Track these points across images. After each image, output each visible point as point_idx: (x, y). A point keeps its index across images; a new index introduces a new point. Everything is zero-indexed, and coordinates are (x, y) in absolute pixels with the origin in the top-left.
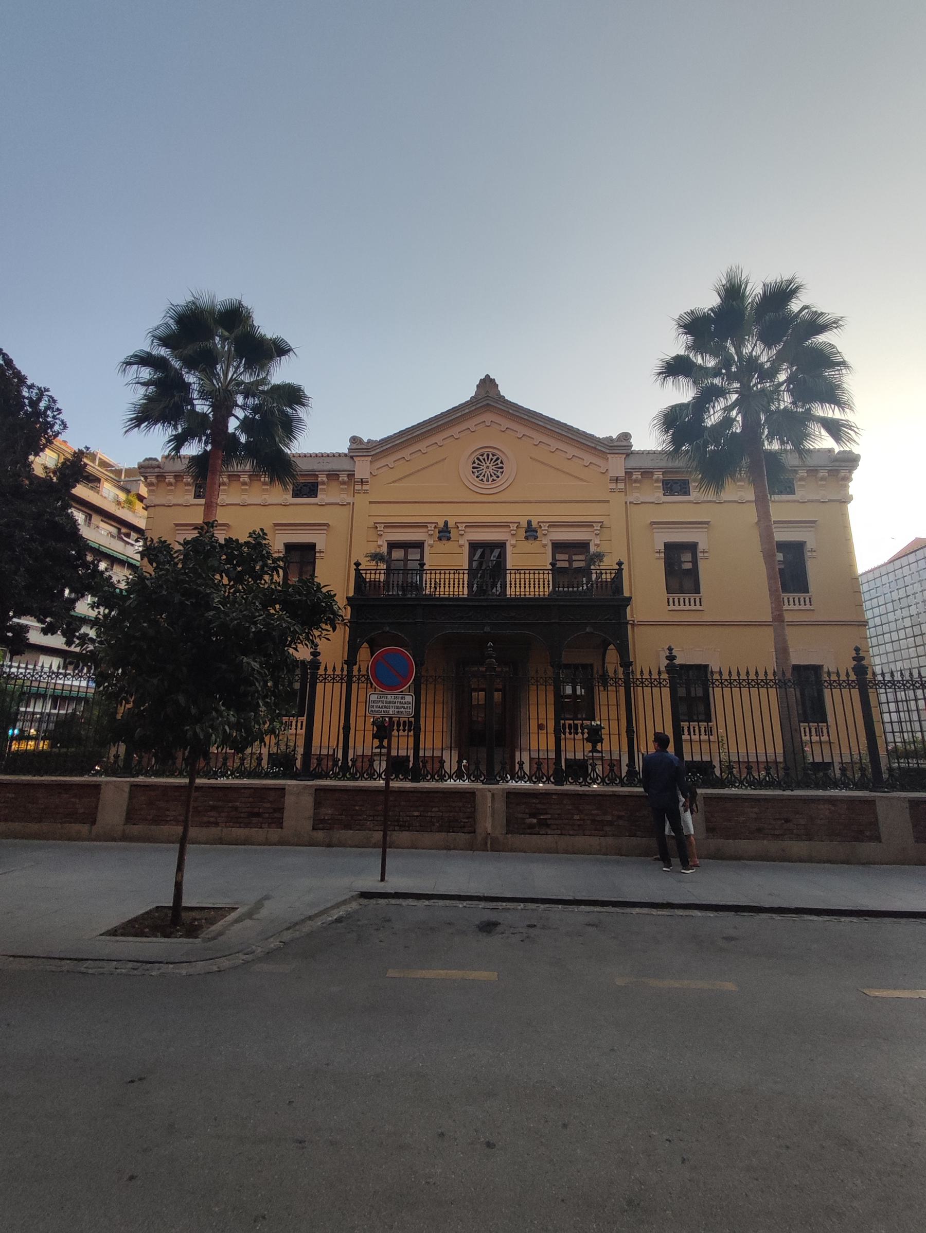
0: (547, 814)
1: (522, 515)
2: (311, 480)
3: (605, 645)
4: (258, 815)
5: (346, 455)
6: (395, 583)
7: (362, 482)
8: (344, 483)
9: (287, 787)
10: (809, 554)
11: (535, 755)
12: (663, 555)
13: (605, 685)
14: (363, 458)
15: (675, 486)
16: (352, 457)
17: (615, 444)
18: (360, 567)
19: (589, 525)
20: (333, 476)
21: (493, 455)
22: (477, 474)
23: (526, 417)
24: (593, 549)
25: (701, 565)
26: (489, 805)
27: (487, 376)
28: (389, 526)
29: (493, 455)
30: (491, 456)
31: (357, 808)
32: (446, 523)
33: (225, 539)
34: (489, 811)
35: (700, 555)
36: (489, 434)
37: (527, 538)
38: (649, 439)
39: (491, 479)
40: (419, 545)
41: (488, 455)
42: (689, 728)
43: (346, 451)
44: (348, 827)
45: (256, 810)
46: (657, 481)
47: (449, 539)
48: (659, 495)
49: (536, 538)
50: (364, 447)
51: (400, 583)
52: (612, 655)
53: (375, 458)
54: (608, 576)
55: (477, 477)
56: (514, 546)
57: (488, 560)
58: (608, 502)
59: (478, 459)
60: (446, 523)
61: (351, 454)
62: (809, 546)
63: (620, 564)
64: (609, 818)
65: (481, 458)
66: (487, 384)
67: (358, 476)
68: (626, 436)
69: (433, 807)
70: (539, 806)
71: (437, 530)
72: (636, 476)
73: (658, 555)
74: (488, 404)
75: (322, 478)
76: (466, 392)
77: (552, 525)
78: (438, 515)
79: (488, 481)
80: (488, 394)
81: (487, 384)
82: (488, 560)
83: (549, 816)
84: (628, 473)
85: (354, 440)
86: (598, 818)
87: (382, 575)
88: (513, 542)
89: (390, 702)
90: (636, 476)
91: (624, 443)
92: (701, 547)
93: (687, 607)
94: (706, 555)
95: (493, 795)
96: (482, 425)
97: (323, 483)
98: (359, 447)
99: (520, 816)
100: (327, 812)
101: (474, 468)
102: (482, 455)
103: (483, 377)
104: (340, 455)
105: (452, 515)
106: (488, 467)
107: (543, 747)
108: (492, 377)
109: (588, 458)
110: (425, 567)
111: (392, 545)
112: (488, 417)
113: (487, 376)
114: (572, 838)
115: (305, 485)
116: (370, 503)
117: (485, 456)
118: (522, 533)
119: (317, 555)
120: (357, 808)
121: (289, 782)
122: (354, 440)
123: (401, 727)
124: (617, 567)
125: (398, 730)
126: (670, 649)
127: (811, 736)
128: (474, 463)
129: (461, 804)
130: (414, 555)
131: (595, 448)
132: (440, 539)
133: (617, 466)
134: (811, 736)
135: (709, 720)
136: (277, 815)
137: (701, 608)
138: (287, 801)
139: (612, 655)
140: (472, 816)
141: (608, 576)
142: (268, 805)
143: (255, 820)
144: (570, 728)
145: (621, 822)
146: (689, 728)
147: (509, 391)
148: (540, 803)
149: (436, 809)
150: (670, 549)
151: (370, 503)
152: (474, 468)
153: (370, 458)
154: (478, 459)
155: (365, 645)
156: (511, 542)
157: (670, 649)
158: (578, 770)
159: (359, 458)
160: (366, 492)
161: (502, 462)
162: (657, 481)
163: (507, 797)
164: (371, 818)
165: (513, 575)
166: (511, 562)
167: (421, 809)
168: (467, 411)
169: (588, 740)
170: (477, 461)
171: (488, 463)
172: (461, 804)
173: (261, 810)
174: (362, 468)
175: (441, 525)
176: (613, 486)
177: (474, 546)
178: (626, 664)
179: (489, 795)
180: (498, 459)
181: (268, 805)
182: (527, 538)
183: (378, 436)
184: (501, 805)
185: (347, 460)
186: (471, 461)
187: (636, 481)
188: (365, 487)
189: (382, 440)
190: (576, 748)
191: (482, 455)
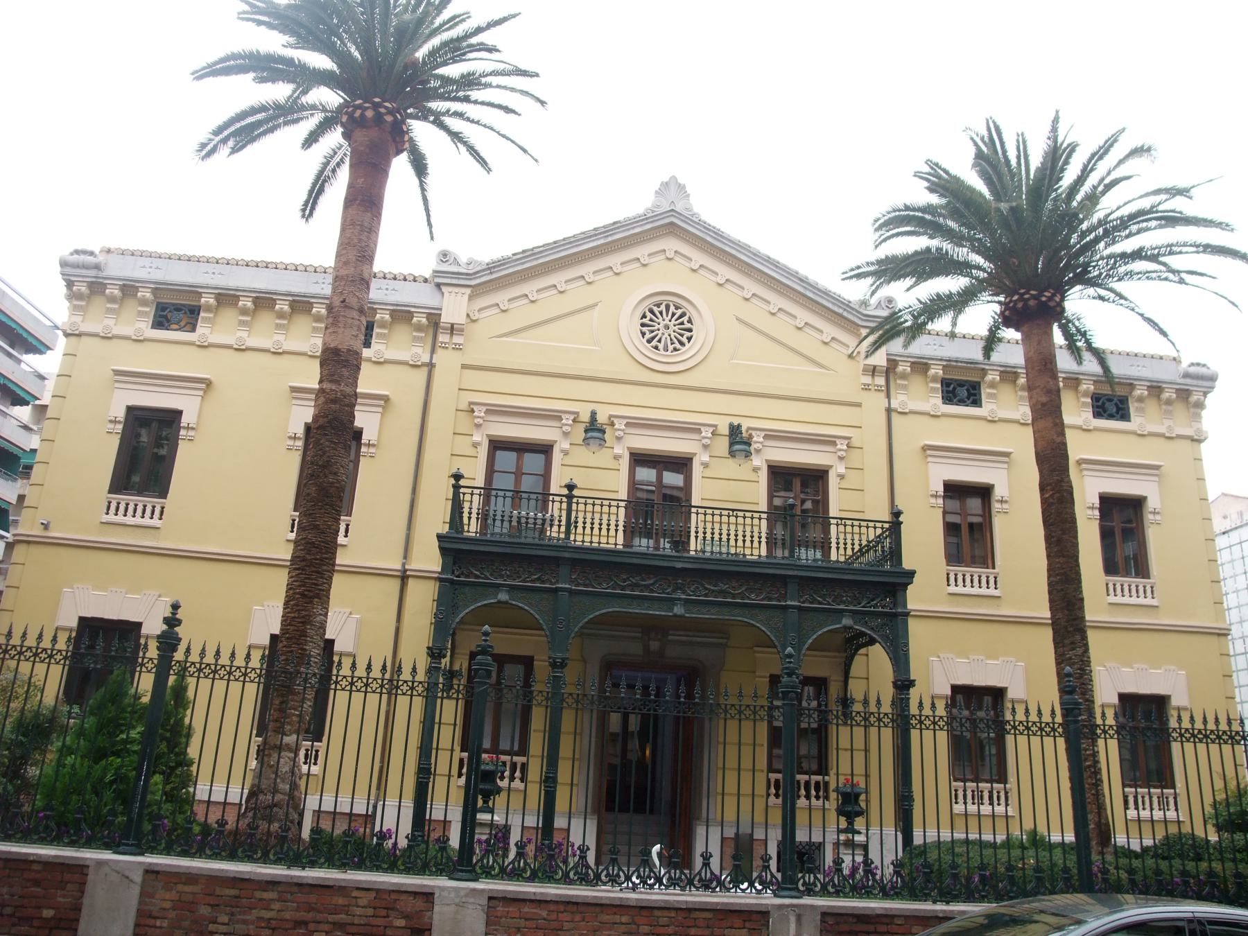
1: (720, 412)
3: (854, 643)
5: (426, 281)
6: (499, 514)
7: (452, 329)
8: (419, 328)
10: (1151, 517)
14: (456, 290)
18: (462, 482)
19: (829, 441)
21: (677, 308)
25: (998, 522)
27: (674, 178)
28: (494, 411)
29: (677, 308)
30: (672, 309)
32: (593, 414)
37: (732, 454)
39: (671, 348)
40: (545, 449)
41: (668, 307)
42: (991, 793)
46: (934, 379)
48: (935, 402)
49: (748, 455)
53: (478, 291)
54: (871, 530)
58: (859, 405)
59: (652, 311)
60: (593, 414)
61: (437, 280)
62: (1152, 503)
67: (446, 318)
72: (903, 368)
73: (933, 500)
74: (672, 224)
77: (771, 436)
78: (579, 399)
87: (476, 498)
88: (705, 458)
92: (998, 492)
93: (976, 591)
94: (1005, 506)
97: (383, 326)
102: (658, 306)
105: (610, 403)
112: (671, 244)
113: (674, 178)
116: (464, 367)
117: (663, 308)
118: (723, 445)
119: (363, 449)
121: (442, 882)
127: (1152, 809)
128: (644, 316)
130: (533, 462)
134: (1152, 809)
135: (1003, 779)
138: (436, 917)
146: (991, 793)
150: (954, 490)
151: (464, 367)
152: (643, 325)
153: (468, 291)
154: (652, 311)
156: (701, 458)
159: (450, 289)
160: (458, 348)
161: (690, 321)
162: (934, 379)
165: (701, 517)
170: (649, 315)
171: (667, 321)
174: (454, 307)
175: (585, 417)
182: (732, 454)
185: (429, 288)
186: (639, 314)
187: (904, 376)
188: (457, 339)
191: (658, 306)
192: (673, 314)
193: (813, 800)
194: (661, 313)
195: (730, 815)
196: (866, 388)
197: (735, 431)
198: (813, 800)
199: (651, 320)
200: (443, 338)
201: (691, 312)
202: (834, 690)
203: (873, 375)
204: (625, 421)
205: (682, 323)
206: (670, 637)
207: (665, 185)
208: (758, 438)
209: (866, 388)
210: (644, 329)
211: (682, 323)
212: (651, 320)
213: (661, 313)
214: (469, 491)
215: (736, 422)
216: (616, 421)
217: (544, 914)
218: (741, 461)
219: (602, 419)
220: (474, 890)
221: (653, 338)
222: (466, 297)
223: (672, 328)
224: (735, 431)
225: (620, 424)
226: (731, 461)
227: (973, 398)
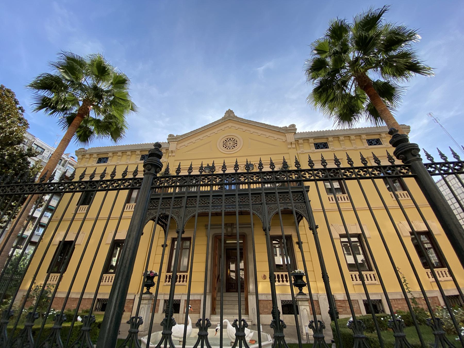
27: (229, 109)
36: (231, 130)
46: (311, 143)
58: (289, 153)
66: (229, 113)
68: (293, 126)
72: (301, 141)
76: (220, 116)
81: (229, 113)
84: (297, 141)
90: (301, 141)
91: (293, 128)
96: (228, 128)
98: (172, 138)
109: (276, 136)
112: (230, 124)
113: (229, 109)
116: (175, 160)
131: (279, 132)
144: (282, 278)
147: (238, 114)
151: (175, 160)
160: (174, 156)
174: (173, 146)
176: (290, 146)
186: (222, 141)
187: (301, 144)
188: (173, 154)
200: (170, 154)
201: (237, 139)
202: (295, 240)
209: (290, 148)
227: (325, 146)
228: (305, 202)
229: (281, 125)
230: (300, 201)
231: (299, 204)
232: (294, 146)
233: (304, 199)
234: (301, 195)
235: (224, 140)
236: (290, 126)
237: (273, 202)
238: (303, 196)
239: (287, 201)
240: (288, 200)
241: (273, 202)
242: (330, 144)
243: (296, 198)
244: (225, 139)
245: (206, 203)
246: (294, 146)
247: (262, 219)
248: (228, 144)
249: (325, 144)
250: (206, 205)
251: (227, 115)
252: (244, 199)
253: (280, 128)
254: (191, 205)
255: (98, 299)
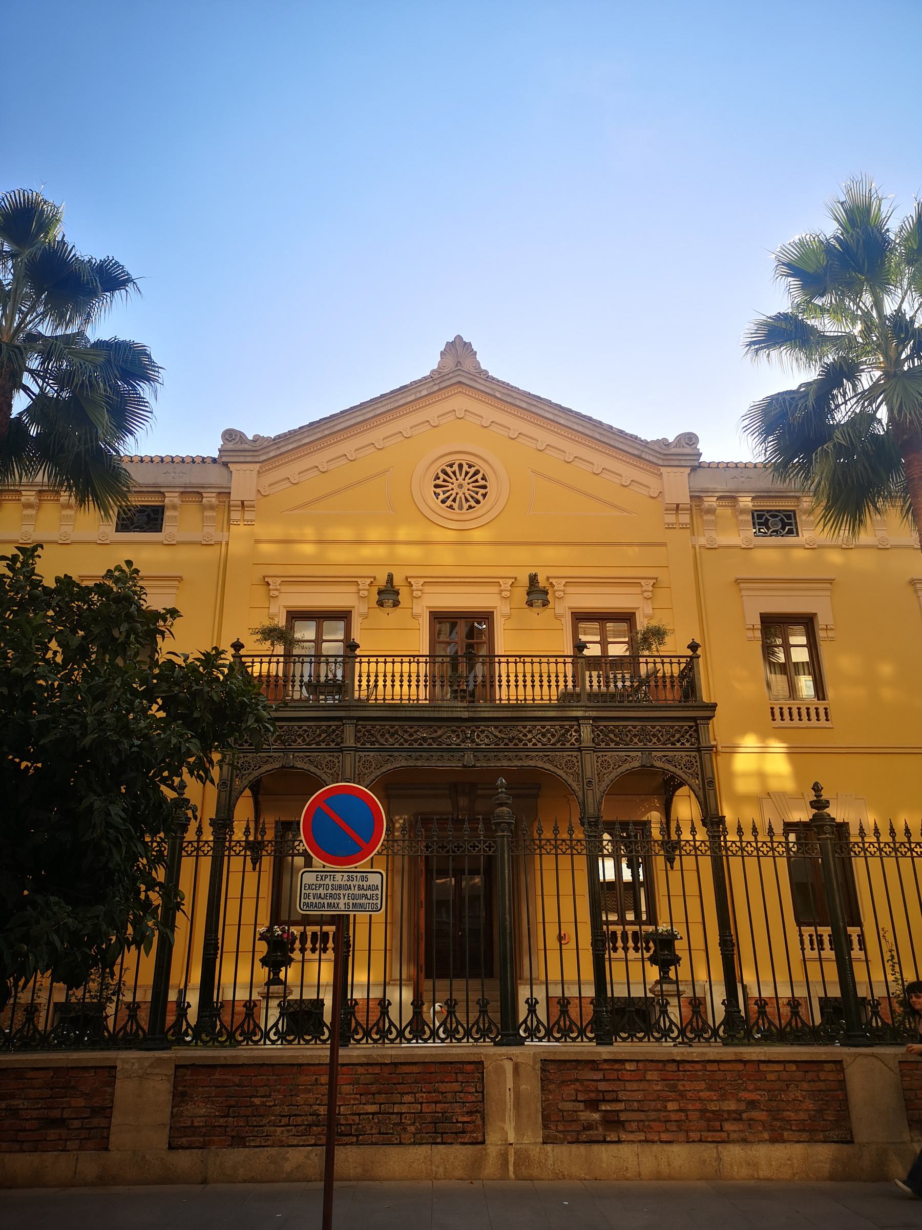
0: (617, 1100)
2: (152, 501)
4: (61, 1122)
5: (214, 460)
9: (119, 1065)
11: (556, 992)
12: (758, 634)
13: (670, 860)
15: (775, 521)
16: (225, 464)
17: (673, 451)
18: (242, 652)
20: (192, 493)
21: (470, 466)
22: (442, 497)
23: (524, 405)
24: (642, 624)
26: (510, 1084)
27: (459, 337)
29: (470, 466)
30: (465, 468)
31: (257, 1101)
32: (390, 578)
33: (58, 580)
34: (509, 1098)
35: (821, 634)
37: (530, 604)
38: (733, 443)
39: (466, 506)
40: (344, 616)
41: (460, 466)
43: (216, 455)
44: (239, 1141)
45: (56, 1114)
46: (743, 512)
47: (396, 604)
49: (545, 603)
50: (246, 447)
51: (306, 679)
52: (686, 809)
55: (443, 502)
56: (508, 617)
57: (463, 638)
58: (664, 544)
60: (390, 578)
61: (224, 459)
63: (694, 647)
64: (732, 1105)
65: (449, 470)
66: (459, 350)
68: (690, 439)
69: (402, 1094)
70: (602, 1086)
71: (375, 590)
72: (710, 501)
73: (750, 634)
74: (460, 382)
75: (171, 498)
76: (423, 363)
77: (571, 582)
79: (461, 508)
80: (459, 369)
81: (459, 350)
82: (463, 638)
83: (621, 1106)
84: (696, 498)
85: (230, 435)
86: (712, 1107)
89: (340, 887)
91: (688, 450)
92: (822, 621)
95: (516, 1068)
96: (451, 417)
97: (174, 507)
99: (569, 1106)
100: (199, 1111)
101: (436, 486)
102: (451, 466)
103: (451, 339)
104: (203, 460)
106: (460, 486)
107: (571, 974)
108: (466, 340)
110: (358, 652)
111: (295, 616)
112: (459, 402)
113: (459, 337)
114: (667, 1147)
115: (143, 510)
117: (456, 467)
118: (521, 594)
120: (257, 1101)
122: (230, 435)
123: (309, 945)
124: (690, 653)
125: (303, 950)
126: (817, 788)
129: (456, 1086)
131: (640, 457)
132: (381, 604)
133: (677, 485)
136: (95, 1122)
137: (828, 724)
138: (118, 1093)
139: (686, 809)
140: (479, 1112)
141: (675, 666)
142: (80, 1102)
143: (53, 1134)
145: (755, 1114)
147: (494, 362)
148: (604, 1080)
149: (408, 1098)
152: (436, 486)
153: (257, 466)
155: (247, 792)
157: (817, 788)
158: (636, 1016)
161: (484, 478)
163: (543, 1070)
164: (284, 1121)
166: (503, 644)
167: (382, 1098)
168: (424, 393)
169: (653, 960)
170: (442, 476)
172: (456, 1086)
173: (65, 1115)
175: (382, 581)
176: (671, 518)
177: (438, 618)
178: (713, 821)
179: (509, 1066)
180: (477, 473)
181: (80, 1102)
182: (530, 604)
183: (271, 432)
184: (531, 1086)
185: (216, 468)
188: (248, 516)
189: (279, 437)
190: (634, 977)
192: (467, 473)
193: (631, 952)
194: (454, 473)
195: (554, 975)
196: (670, 527)
197: (533, 579)
198: (631, 952)
199: (444, 481)
200: (235, 515)
201: (484, 468)
203: (677, 513)
204: (422, 581)
205: (476, 481)
206: (479, 792)
207: (451, 346)
208: (559, 584)
209: (670, 527)
210: (438, 490)
211: (476, 481)
212: (444, 481)
213: (454, 473)
214: (250, 659)
215: (533, 571)
216: (412, 580)
217: (237, 1079)
218: (541, 610)
219: (397, 581)
220: (160, 1059)
221: (448, 498)
222: (255, 473)
223: (466, 487)
224: (533, 579)
225: (417, 584)
226: (528, 611)
228: (699, 750)
229: (648, 434)
230: (688, 745)
231: (683, 754)
232: (685, 518)
233: (698, 739)
234: (691, 727)
235: (436, 468)
236: (680, 438)
237: (612, 745)
238: (697, 731)
239: (650, 745)
240: (654, 740)
241: (612, 745)
242: (802, 518)
243: (677, 736)
244: (442, 463)
245: (416, 741)
246: (685, 518)
247: (580, 794)
248: (453, 485)
249: (789, 517)
250: (416, 746)
251: (451, 364)
252: (530, 732)
253: (645, 444)
254: (372, 743)
255: (55, 1003)
